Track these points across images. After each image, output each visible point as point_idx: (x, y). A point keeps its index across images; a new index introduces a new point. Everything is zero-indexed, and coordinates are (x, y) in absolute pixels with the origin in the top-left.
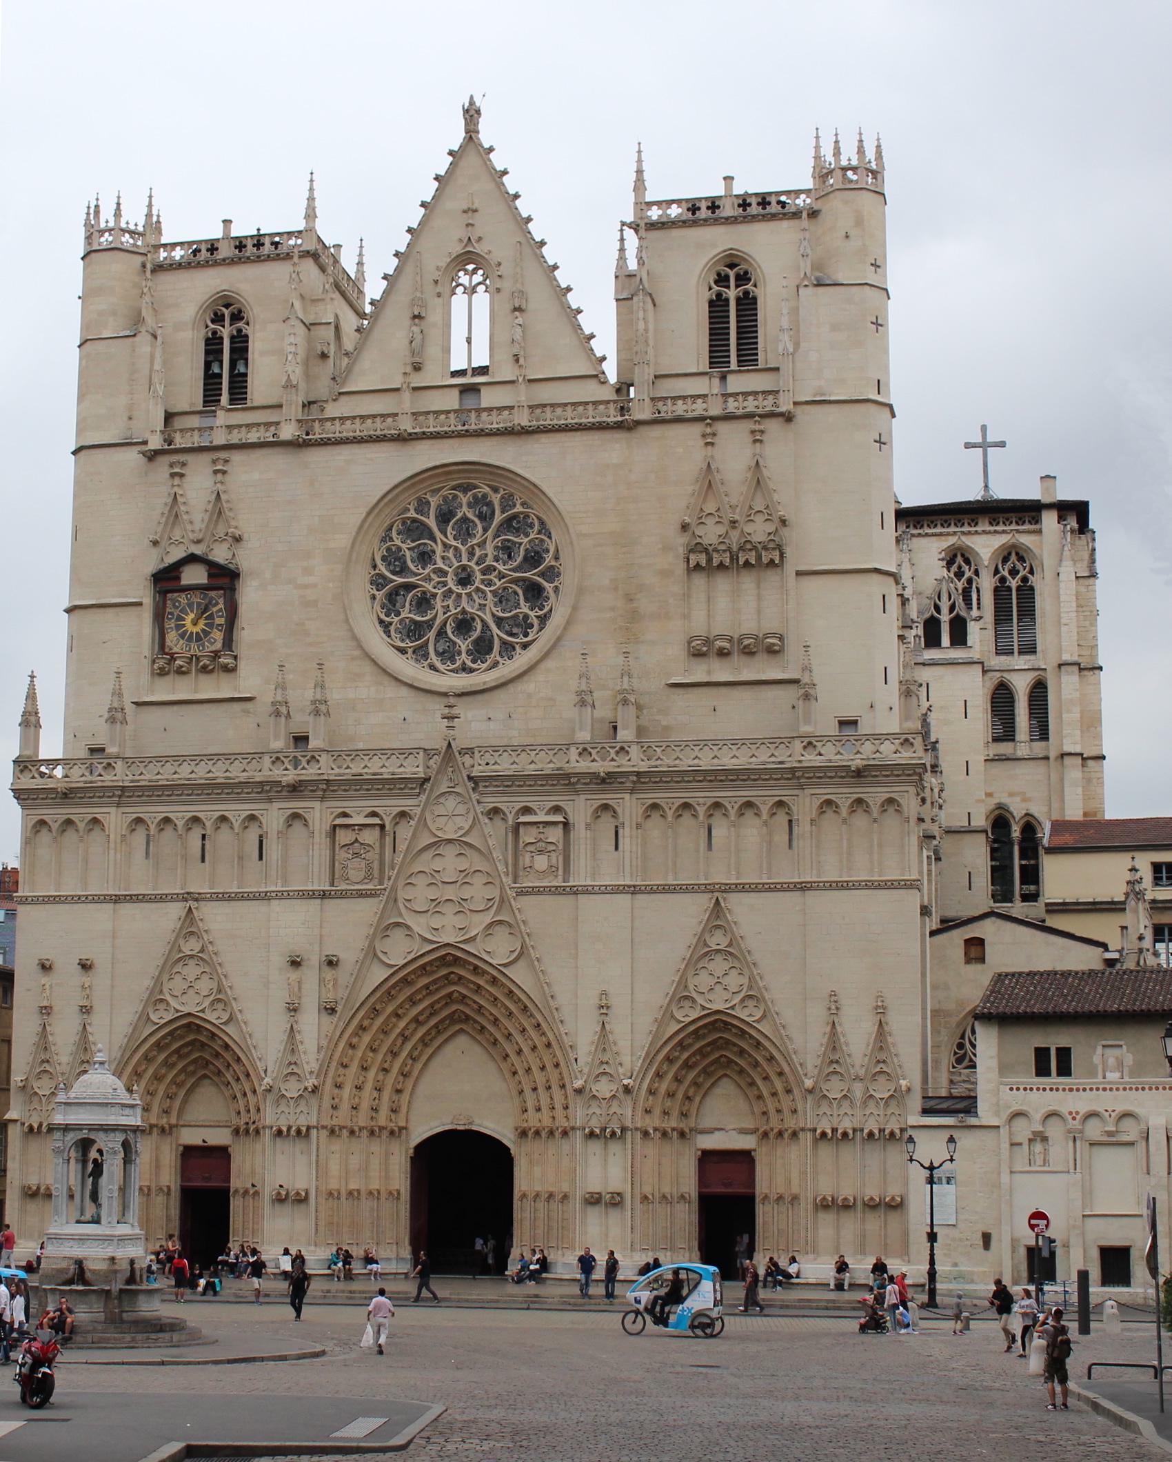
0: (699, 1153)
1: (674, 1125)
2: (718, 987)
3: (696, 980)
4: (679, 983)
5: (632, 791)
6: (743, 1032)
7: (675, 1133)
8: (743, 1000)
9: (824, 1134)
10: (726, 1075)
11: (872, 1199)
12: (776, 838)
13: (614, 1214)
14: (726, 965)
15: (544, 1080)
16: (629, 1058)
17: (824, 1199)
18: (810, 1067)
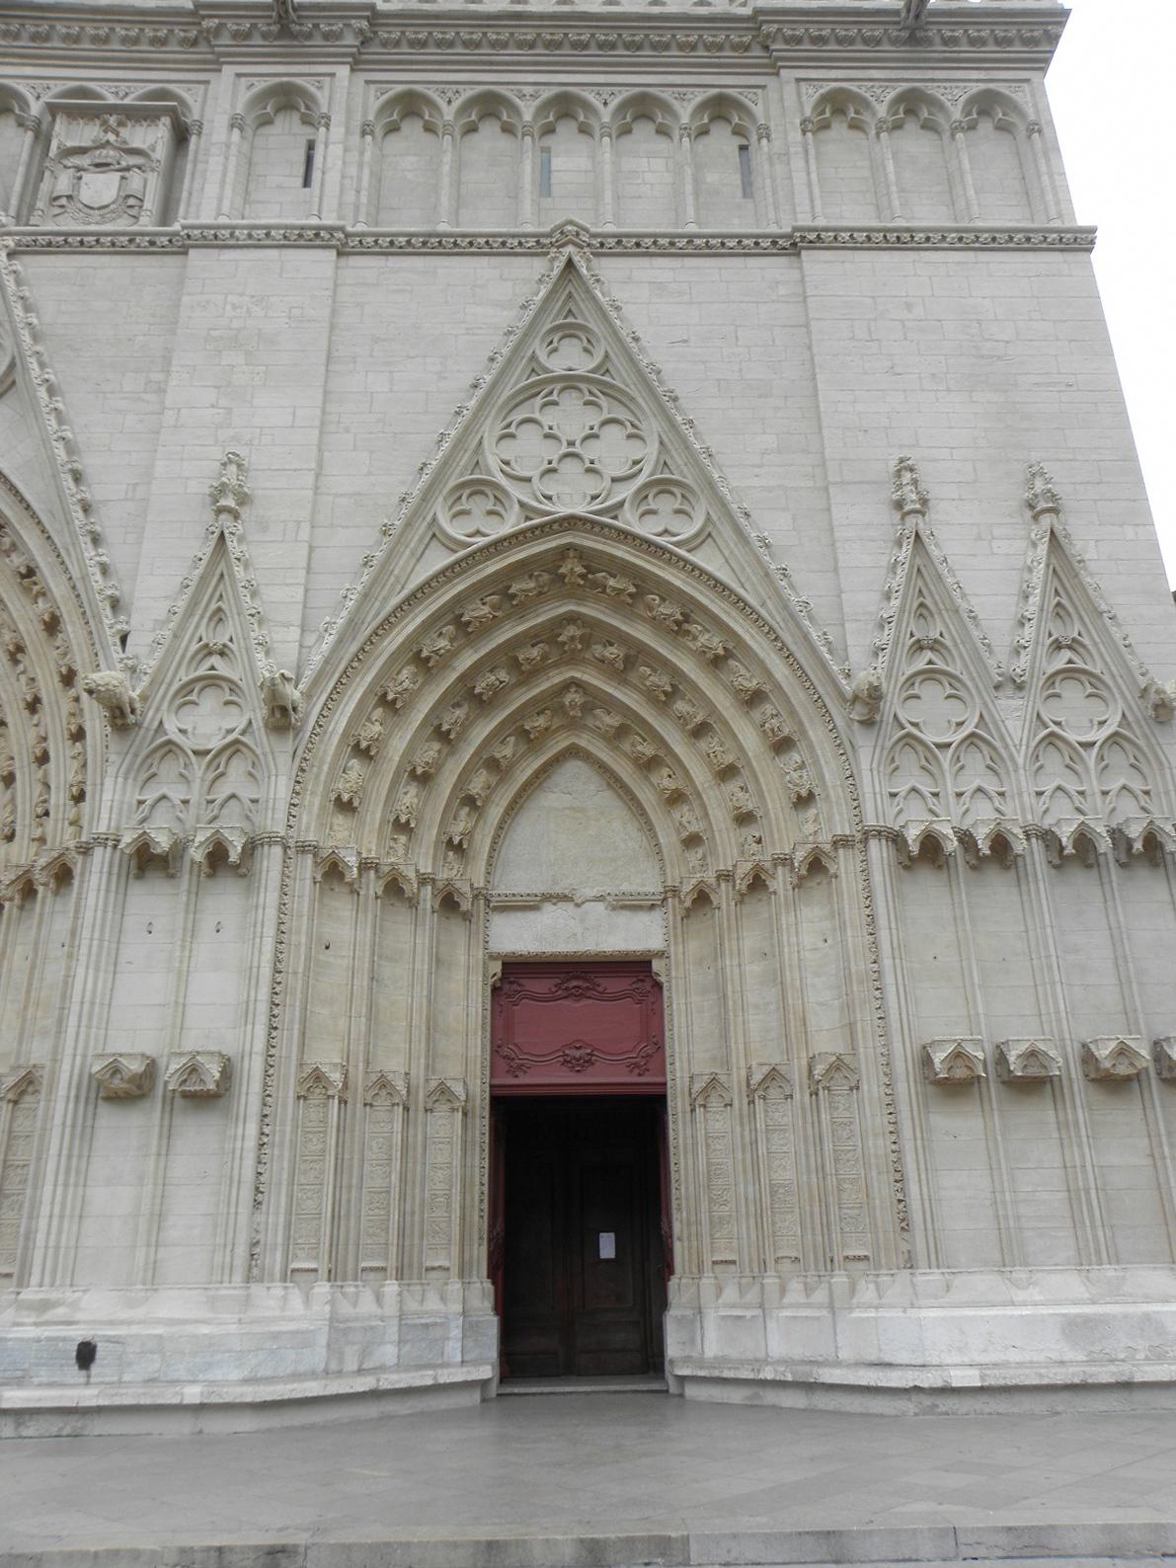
0: (496, 967)
1: (426, 867)
2: (570, 467)
3: (508, 450)
4: (459, 444)
5: (356, 65)
6: (644, 583)
7: (428, 891)
8: (641, 495)
9: (931, 846)
10: (573, 752)
11: (1123, 1051)
12: (712, 178)
13: (197, 1136)
14: (594, 418)
15: (32, 735)
16: (294, 633)
17: (958, 1055)
18: (857, 655)
